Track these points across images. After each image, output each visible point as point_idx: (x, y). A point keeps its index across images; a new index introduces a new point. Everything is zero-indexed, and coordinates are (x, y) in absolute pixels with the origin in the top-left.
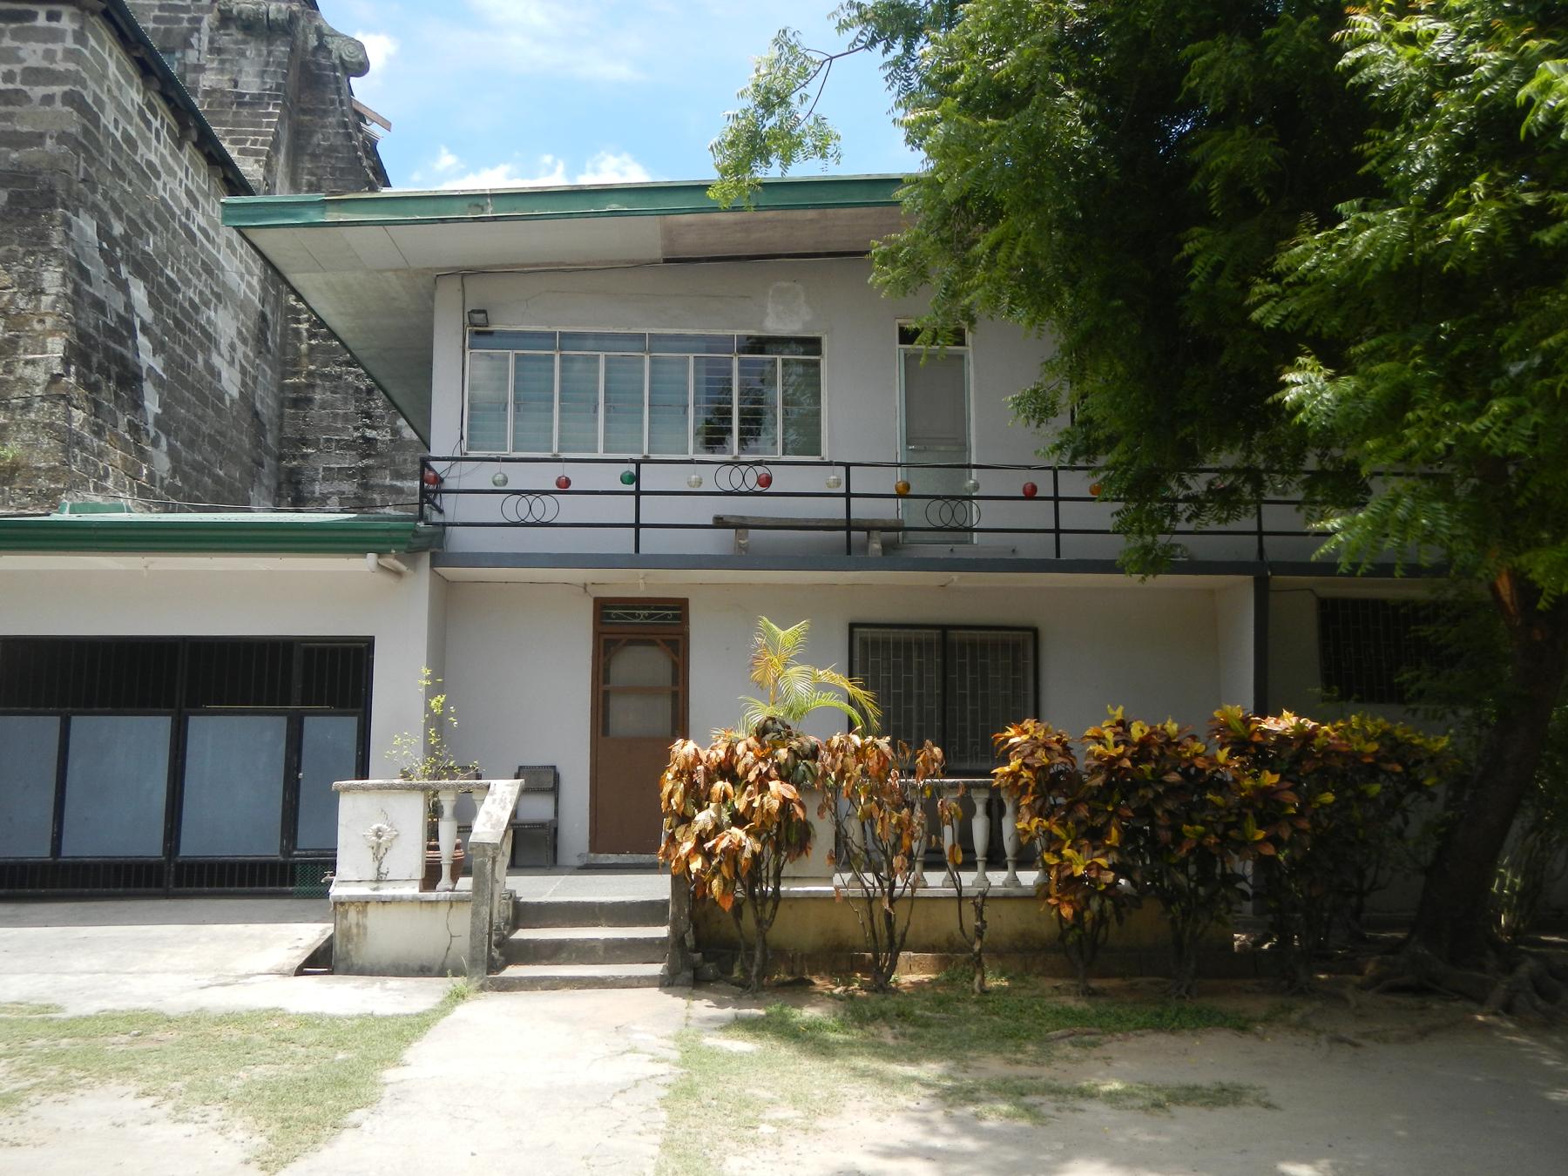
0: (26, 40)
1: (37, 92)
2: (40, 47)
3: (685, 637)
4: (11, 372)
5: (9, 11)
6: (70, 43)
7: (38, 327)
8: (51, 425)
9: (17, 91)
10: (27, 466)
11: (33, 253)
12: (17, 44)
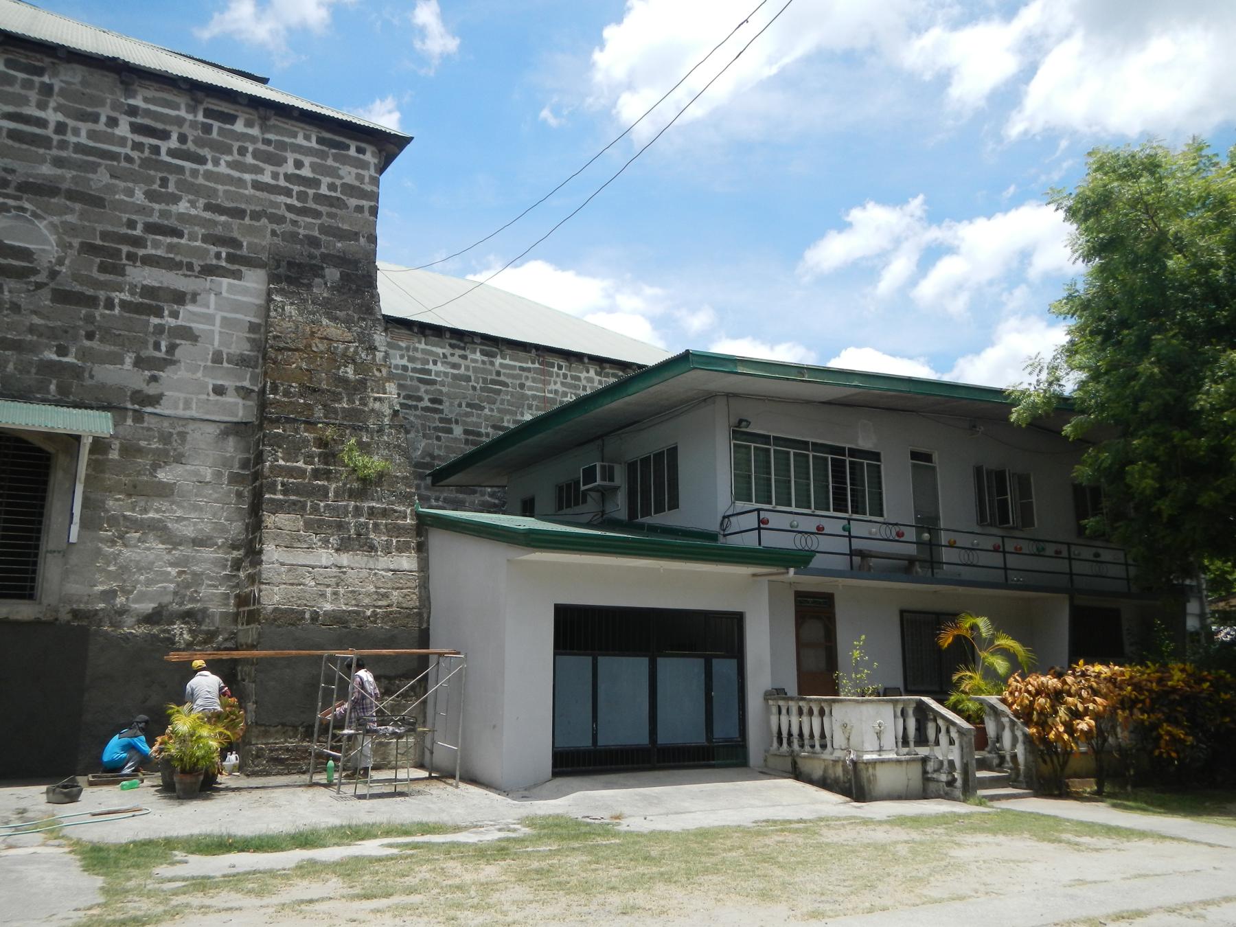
0: (344, 164)
1: (353, 202)
2: (354, 171)
3: (834, 614)
4: (365, 405)
5: (331, 140)
6: (372, 172)
7: (377, 374)
8: (399, 446)
9: (338, 199)
10: (388, 474)
11: (364, 319)
12: (337, 165)
